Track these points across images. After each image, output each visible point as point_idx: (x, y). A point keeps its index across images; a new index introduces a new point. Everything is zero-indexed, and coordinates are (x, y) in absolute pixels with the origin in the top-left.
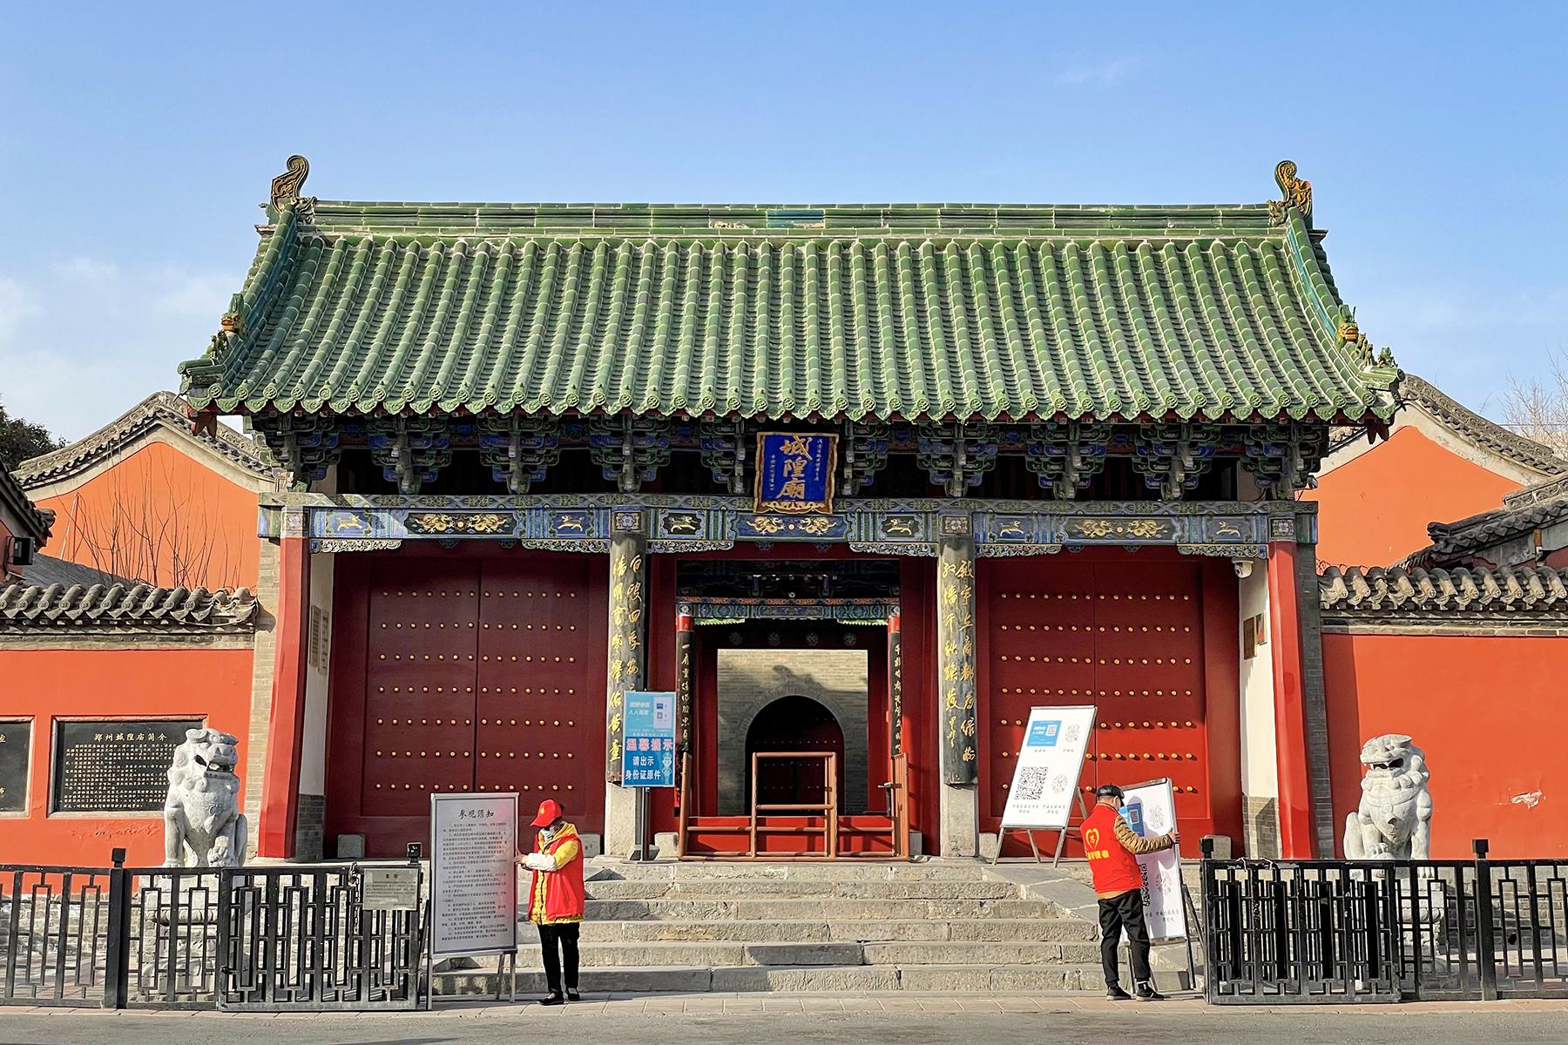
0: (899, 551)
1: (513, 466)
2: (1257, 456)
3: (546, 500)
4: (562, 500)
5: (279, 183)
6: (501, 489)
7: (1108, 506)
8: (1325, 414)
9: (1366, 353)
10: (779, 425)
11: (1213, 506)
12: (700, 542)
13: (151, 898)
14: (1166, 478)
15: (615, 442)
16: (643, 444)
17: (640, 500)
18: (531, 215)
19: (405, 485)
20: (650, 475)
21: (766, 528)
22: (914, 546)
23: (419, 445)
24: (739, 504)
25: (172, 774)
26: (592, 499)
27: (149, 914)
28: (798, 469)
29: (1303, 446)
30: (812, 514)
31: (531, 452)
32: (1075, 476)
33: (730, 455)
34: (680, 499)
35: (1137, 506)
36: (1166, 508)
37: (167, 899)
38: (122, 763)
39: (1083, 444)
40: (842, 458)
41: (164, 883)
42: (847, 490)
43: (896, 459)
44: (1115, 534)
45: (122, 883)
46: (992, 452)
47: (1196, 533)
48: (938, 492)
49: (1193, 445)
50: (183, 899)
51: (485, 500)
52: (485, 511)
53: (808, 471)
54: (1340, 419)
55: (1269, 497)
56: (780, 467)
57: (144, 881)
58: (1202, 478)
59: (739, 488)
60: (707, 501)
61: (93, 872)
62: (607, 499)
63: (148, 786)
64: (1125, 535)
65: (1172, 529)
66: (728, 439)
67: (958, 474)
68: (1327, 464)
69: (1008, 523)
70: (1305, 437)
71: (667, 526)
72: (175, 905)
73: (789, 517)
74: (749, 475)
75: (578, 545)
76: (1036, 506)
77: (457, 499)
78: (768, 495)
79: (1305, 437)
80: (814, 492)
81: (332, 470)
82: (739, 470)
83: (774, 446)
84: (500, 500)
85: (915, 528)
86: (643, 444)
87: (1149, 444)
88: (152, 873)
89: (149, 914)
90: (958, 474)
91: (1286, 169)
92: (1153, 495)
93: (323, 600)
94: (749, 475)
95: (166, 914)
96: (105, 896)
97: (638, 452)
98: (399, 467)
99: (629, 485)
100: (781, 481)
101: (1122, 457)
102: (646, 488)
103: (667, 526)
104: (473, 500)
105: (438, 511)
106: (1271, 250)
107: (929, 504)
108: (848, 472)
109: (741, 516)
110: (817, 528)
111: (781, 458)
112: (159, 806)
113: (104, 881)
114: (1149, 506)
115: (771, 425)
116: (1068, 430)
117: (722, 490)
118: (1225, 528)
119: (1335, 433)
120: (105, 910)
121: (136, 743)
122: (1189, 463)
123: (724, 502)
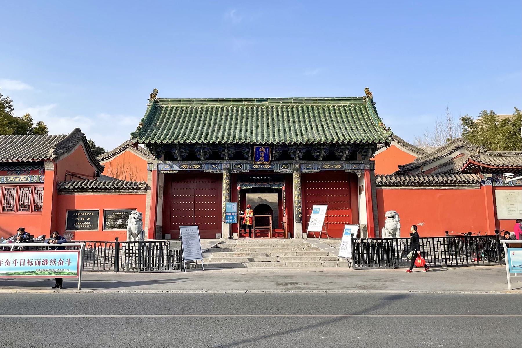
0: (284, 172)
1: (202, 154)
2: (363, 151)
3: (209, 162)
4: (212, 161)
5: (152, 95)
6: (199, 159)
7: (329, 162)
8: (376, 141)
9: (385, 128)
10: (259, 145)
11: (353, 162)
12: (242, 170)
13: (124, 248)
14: (342, 156)
15: (223, 149)
16: (230, 149)
17: (229, 161)
18: (206, 101)
19: (179, 159)
20: (231, 156)
21: (256, 167)
22: (288, 171)
23: (182, 150)
24: (251, 162)
25: (129, 221)
26: (219, 161)
27: (124, 252)
28: (263, 154)
29: (372, 149)
30: (265, 164)
31: (206, 151)
32: (322, 155)
33: (249, 152)
34: (238, 161)
35: (336, 162)
36: (342, 162)
37: (127, 248)
38: (119, 219)
39: (324, 149)
40: (272, 152)
41: (127, 245)
42: (273, 159)
43: (284, 152)
44: (331, 168)
45: (118, 245)
46: (304, 150)
47: (349, 168)
48: (293, 159)
49: (348, 149)
50: (131, 248)
51: (196, 162)
52: (196, 164)
53: (265, 155)
54: (380, 143)
55: (364, 160)
56: (259, 154)
57: (123, 244)
58: (350, 156)
59: (250, 159)
60: (244, 161)
61: (111, 242)
62: (222, 161)
63: (124, 224)
64: (333, 168)
65: (343, 167)
66: (248, 148)
67: (297, 155)
68: (377, 153)
69: (308, 166)
70: (372, 147)
71: (235, 167)
72: (129, 249)
73: (261, 165)
74: (252, 157)
75: (216, 171)
76: (314, 162)
77: (190, 162)
78: (257, 160)
79: (372, 147)
80: (266, 159)
81: (163, 155)
82: (250, 155)
83: (257, 149)
84: (199, 162)
85: (288, 167)
86: (230, 149)
87: (338, 149)
88: (124, 243)
89: (124, 252)
90: (297, 155)
91: (367, 89)
92: (340, 160)
93: (161, 183)
94: (252, 157)
95: (127, 251)
96: (114, 248)
97: (228, 151)
98: (177, 155)
99: (227, 158)
100: (259, 157)
101: (333, 151)
102: (230, 159)
103: (235, 167)
104: (193, 162)
105: (186, 164)
106: (363, 107)
107: (291, 162)
108: (274, 155)
109: (251, 166)
110: (267, 167)
111: (259, 152)
112: (126, 228)
113: (114, 244)
114: (338, 162)
115: (257, 145)
116: (343, 145)
117: (247, 159)
118: (355, 166)
119: (379, 146)
120: (114, 251)
121: (122, 215)
122: (347, 152)
123: (247, 162)
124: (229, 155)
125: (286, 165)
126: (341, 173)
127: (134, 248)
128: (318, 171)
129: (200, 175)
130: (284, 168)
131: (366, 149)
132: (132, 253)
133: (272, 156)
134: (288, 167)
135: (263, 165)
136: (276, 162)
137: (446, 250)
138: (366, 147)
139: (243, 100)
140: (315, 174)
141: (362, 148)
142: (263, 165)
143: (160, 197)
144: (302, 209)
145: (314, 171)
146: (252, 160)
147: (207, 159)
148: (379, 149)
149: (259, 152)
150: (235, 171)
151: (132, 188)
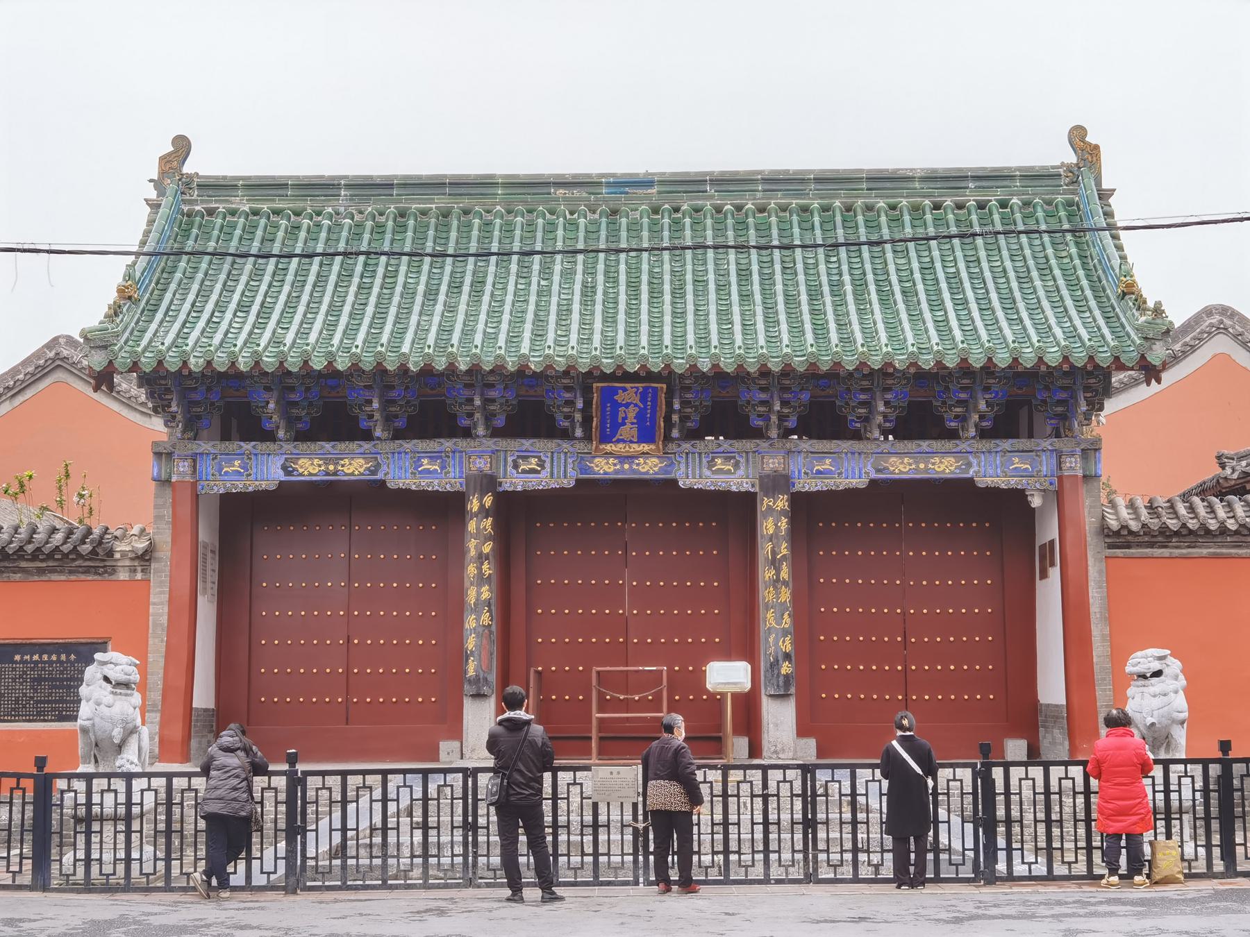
0: (722, 486)
1: (377, 416)
2: (1043, 399)
3: (408, 445)
4: (421, 445)
5: (165, 160)
6: (367, 436)
7: (911, 445)
8: (1104, 358)
9: (1140, 304)
10: (612, 377)
11: (1006, 444)
12: (544, 481)
13: (69, 796)
14: (963, 419)
15: (467, 393)
16: (493, 394)
17: (490, 444)
18: (391, 186)
19: (281, 434)
20: (500, 422)
21: (604, 467)
22: (738, 480)
23: (294, 397)
24: (580, 446)
25: (83, 690)
26: (448, 444)
27: (68, 811)
28: (632, 413)
29: (1087, 389)
30: (645, 454)
31: (392, 402)
32: (880, 419)
33: (571, 403)
34: (527, 444)
35: (937, 445)
36: (963, 446)
37: (82, 799)
38: (39, 680)
39: (887, 389)
40: (669, 404)
41: (80, 785)
42: (675, 433)
43: (718, 403)
44: (917, 470)
45: (44, 785)
46: (805, 397)
47: (993, 467)
48: (759, 434)
49: (987, 389)
50: (96, 798)
51: (353, 446)
52: (352, 455)
53: (640, 417)
54: (1122, 367)
55: (1058, 436)
56: (615, 414)
57: (61, 784)
58: (996, 419)
59: (579, 432)
60: (551, 444)
61: (18, 776)
62: (462, 443)
63: (61, 701)
64: (926, 470)
65: (969, 465)
66: (568, 389)
67: (774, 418)
68: (1112, 406)
69: (821, 460)
70: (1085, 383)
71: (516, 466)
73: (623, 458)
74: (587, 421)
75: (435, 485)
76: (845, 445)
77: (328, 446)
78: (605, 439)
79: (1085, 383)
80: (646, 435)
81: (216, 422)
82: (578, 417)
83: (608, 395)
84: (367, 446)
85: (737, 465)
86: (493, 394)
87: (947, 388)
88: (70, 777)
89: (68, 811)
90: (774, 418)
91: (1077, 136)
92: (953, 435)
94: (587, 421)
95: (82, 811)
96: (30, 796)
97: (487, 401)
98: (275, 418)
99: (481, 430)
100: (616, 426)
101: (924, 401)
102: (496, 433)
103: (516, 466)
104: (342, 446)
105: (310, 456)
106: (1058, 208)
107: (749, 445)
108: (675, 418)
109: (581, 458)
110: (649, 466)
111: (617, 406)
112: (75, 718)
113: (28, 784)
114: (949, 445)
115: (604, 377)
116: (877, 378)
117: (566, 435)
118: (1017, 463)
119: (1117, 378)
120: (29, 808)
121: (50, 663)
122: (982, 406)
123: (566, 445)
124: (489, 417)
125: (727, 459)
126: (958, 497)
127: (109, 799)
128: (859, 482)
129: (371, 498)
130: (720, 471)
131: (1063, 388)
132: (102, 819)
133: (668, 419)
134: (737, 465)
135: (630, 458)
136: (686, 446)
137: (1214, 811)
138: (1066, 382)
139: (547, 184)
140: (851, 493)
141: (1047, 388)
142: (630, 458)
143: (204, 593)
144: (795, 643)
145: (842, 483)
146: (588, 438)
147: (398, 435)
148: (1120, 391)
149: (617, 406)
150: (514, 481)
151: (87, 556)
